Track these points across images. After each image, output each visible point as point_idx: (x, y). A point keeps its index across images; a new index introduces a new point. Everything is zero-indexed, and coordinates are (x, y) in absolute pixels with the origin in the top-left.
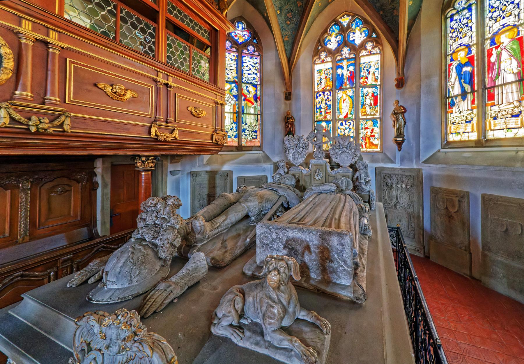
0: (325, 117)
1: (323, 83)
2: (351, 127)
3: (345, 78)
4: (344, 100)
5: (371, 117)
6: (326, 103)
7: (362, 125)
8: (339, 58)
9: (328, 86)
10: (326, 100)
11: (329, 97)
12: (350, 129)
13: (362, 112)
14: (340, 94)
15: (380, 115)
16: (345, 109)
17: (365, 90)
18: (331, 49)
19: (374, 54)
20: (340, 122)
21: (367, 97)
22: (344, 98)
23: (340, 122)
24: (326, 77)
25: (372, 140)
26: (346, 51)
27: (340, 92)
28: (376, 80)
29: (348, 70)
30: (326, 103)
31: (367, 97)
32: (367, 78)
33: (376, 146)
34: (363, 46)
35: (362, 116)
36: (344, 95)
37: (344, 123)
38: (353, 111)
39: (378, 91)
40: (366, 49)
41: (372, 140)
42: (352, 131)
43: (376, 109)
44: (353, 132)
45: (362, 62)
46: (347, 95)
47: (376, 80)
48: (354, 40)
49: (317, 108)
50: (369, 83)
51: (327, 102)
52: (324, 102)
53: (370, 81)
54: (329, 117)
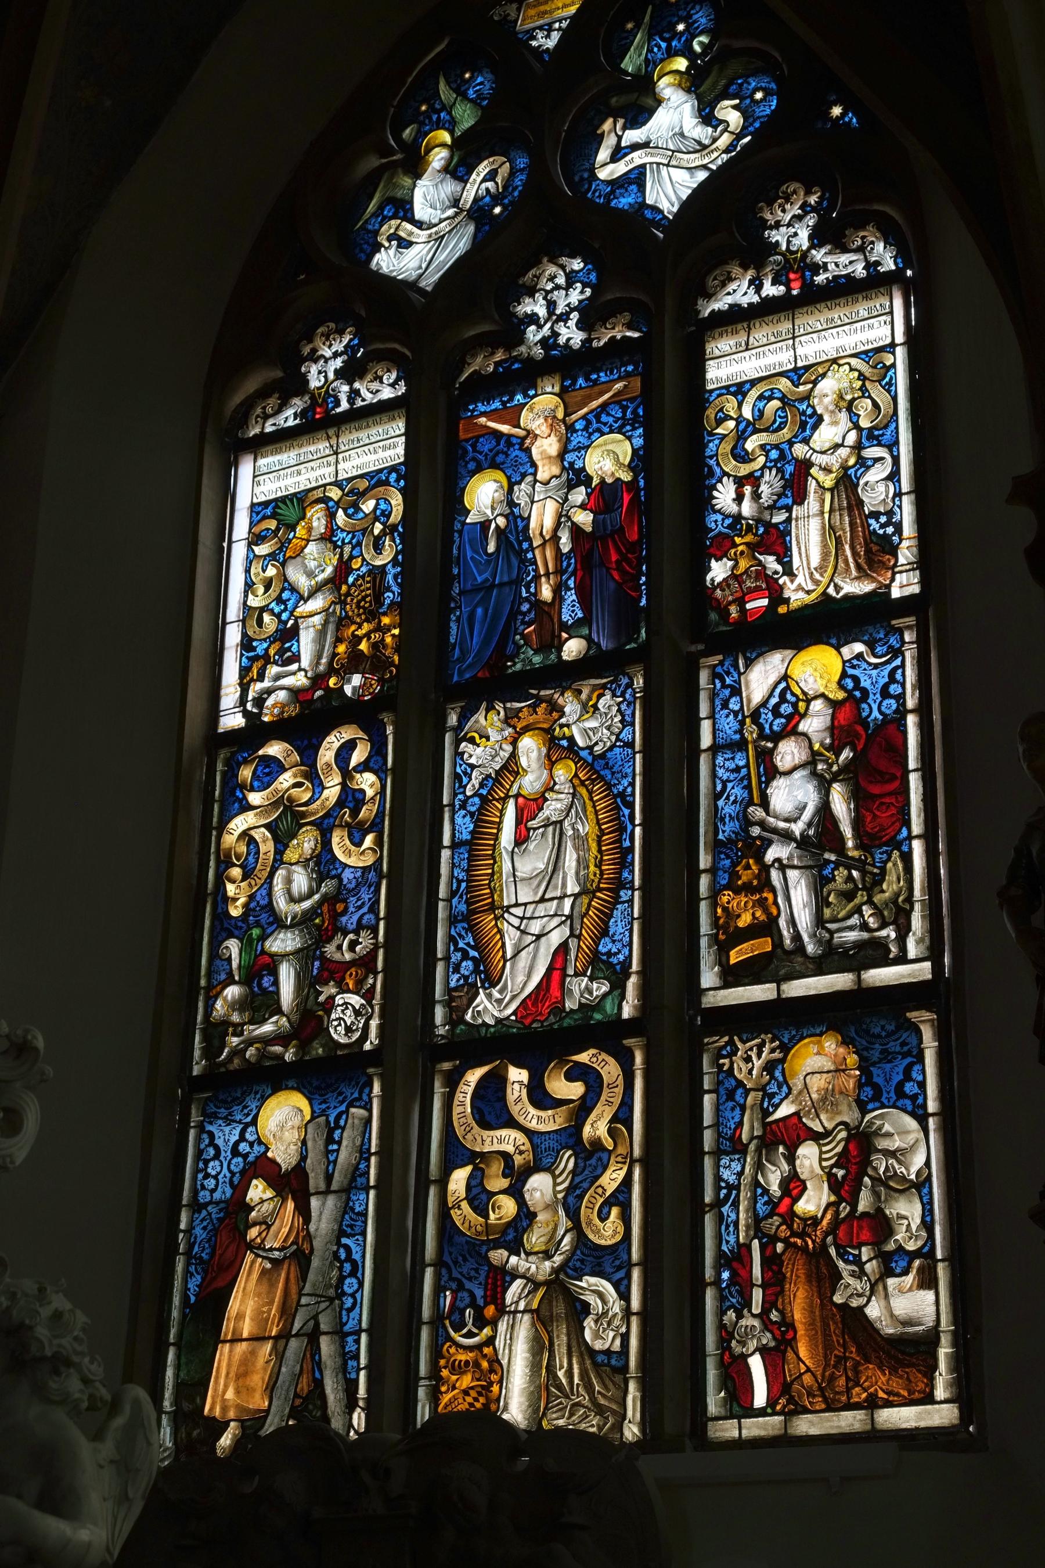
0: (311, 1020)
1: (306, 644)
2: (597, 1127)
3: (544, 559)
4: (529, 808)
5: (839, 981)
6: (323, 863)
7: (730, 1091)
8: (484, 363)
9: (355, 662)
10: (325, 827)
11: (367, 782)
12: (592, 1158)
13: (729, 936)
14: (486, 742)
15: (934, 954)
16: (539, 904)
17: (760, 679)
18: (411, 286)
19: (845, 290)
20: (474, 1076)
21: (789, 753)
22: (530, 782)
23: (474, 1076)
24: (343, 568)
25: (850, 1288)
26: (556, 304)
27: (489, 722)
28: (877, 552)
29: (577, 477)
30: (323, 863)
31: (789, 753)
32: (775, 540)
33: (911, 1352)
34: (726, 217)
35: (731, 977)
36: (530, 747)
37: (517, 1075)
38: (628, 941)
39: (896, 675)
40: (756, 254)
41: (850, 1288)
42: (611, 1179)
43: (891, 886)
44: (620, 1198)
45: (719, 372)
46: (559, 748)
47: (877, 552)
48: (637, 178)
49: (224, 927)
50: (798, 592)
51: (339, 842)
52: (306, 842)
53: (811, 566)
54: (350, 1016)
